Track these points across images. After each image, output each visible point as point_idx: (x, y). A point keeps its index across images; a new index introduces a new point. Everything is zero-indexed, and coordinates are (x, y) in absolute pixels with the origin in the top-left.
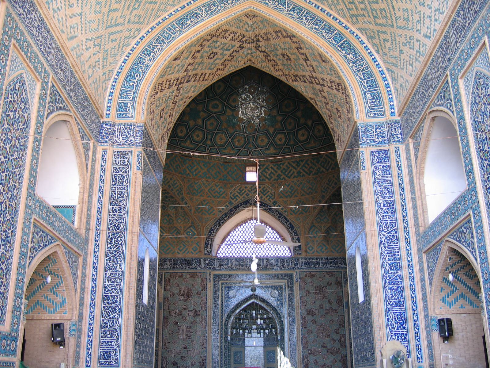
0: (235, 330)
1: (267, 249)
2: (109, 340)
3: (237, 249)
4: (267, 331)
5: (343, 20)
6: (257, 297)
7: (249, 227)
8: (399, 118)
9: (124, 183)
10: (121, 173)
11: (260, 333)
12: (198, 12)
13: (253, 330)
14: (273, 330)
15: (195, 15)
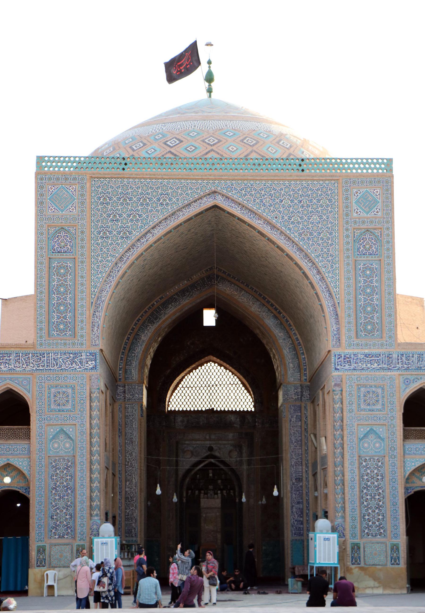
0: (190, 491)
1: (226, 397)
2: (131, 522)
3: (192, 397)
4: (225, 492)
5: (277, 307)
6: (214, 457)
7: (205, 371)
8: (309, 384)
9: (134, 426)
10: (131, 419)
11: (217, 494)
12: (176, 297)
13: (210, 490)
14: (232, 491)
15: (174, 300)
